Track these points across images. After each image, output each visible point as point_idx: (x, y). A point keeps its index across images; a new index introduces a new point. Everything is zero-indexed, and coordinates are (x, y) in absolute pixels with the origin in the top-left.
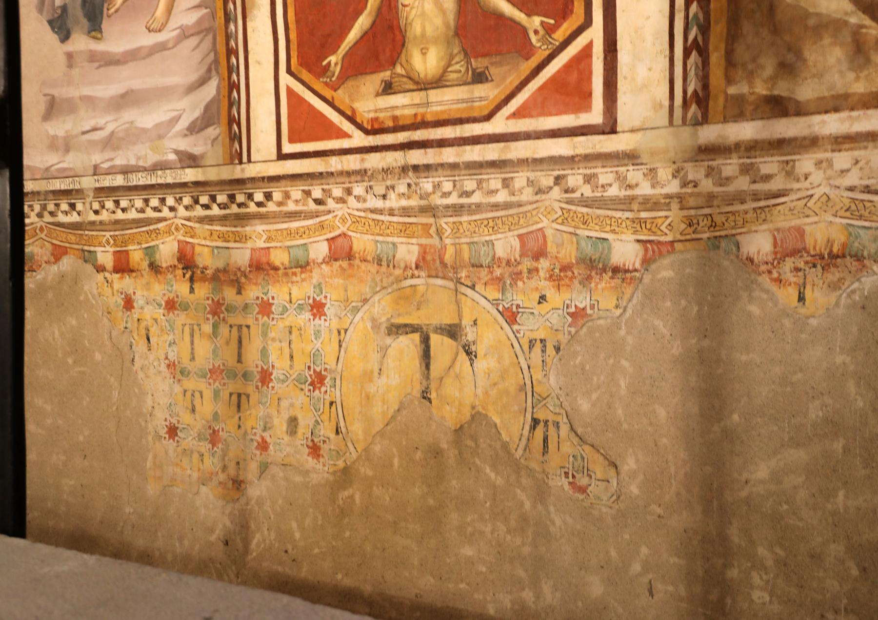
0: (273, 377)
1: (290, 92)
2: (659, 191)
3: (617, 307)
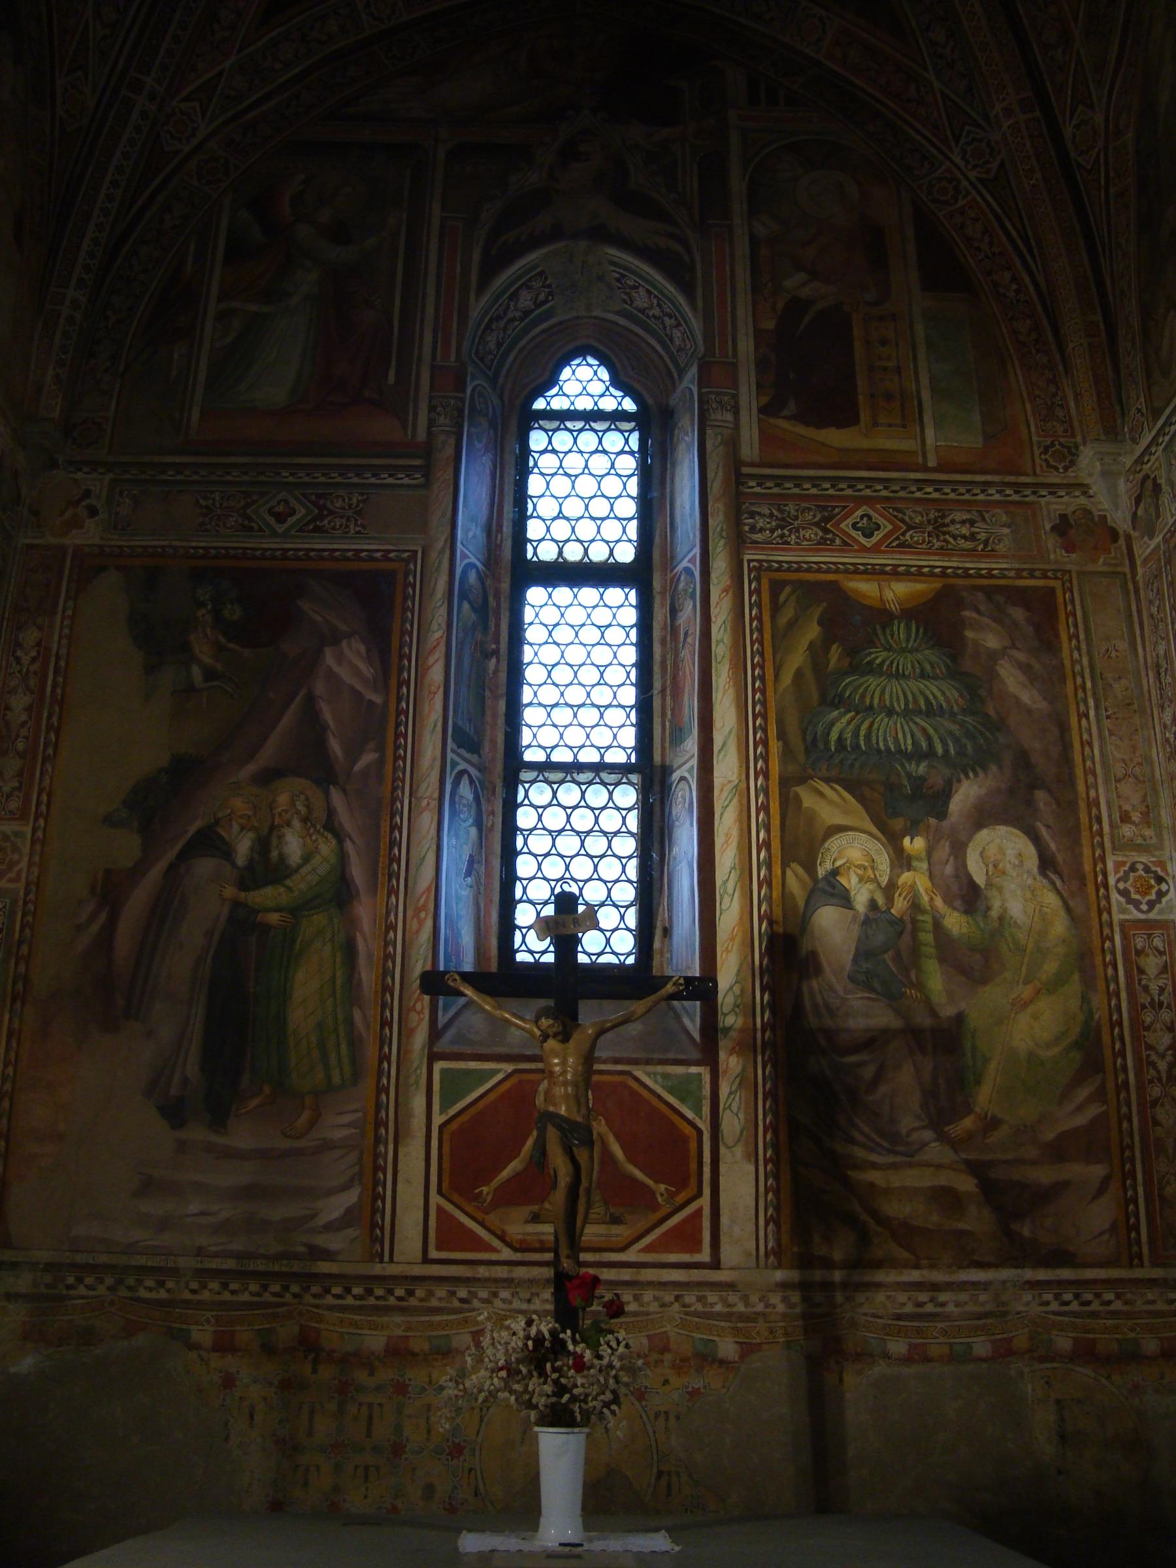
0: (407, 1449)
1: (440, 1209)
2: (750, 1310)
3: (723, 1387)
